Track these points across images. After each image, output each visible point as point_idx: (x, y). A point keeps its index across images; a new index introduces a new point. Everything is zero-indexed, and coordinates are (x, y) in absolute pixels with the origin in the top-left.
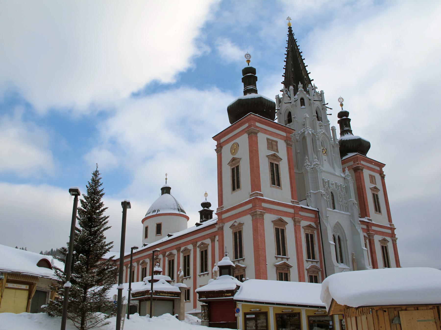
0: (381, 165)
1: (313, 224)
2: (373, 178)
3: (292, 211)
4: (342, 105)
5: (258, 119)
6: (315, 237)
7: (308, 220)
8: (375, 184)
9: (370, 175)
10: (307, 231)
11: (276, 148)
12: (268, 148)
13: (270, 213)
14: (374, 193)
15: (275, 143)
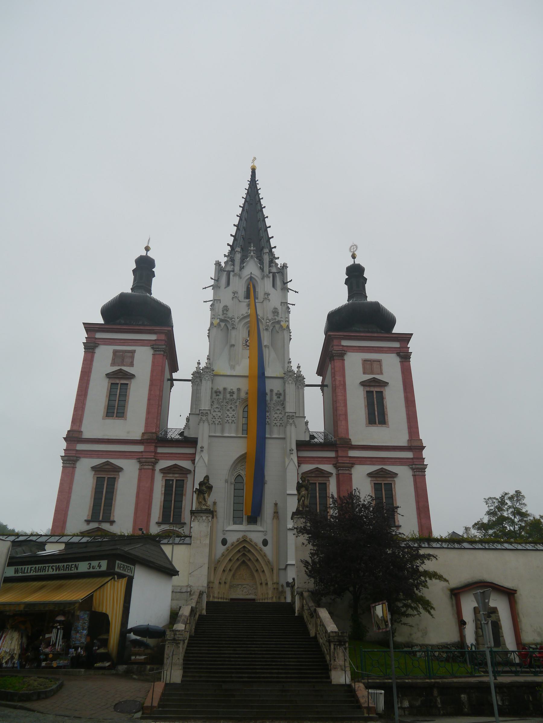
0: (406, 338)
1: (185, 464)
2: (375, 365)
3: (140, 448)
4: (354, 257)
5: (99, 328)
6: (187, 484)
7: (176, 458)
8: (378, 374)
9: (365, 361)
10: (171, 475)
11: (130, 360)
12: (113, 364)
13: (91, 457)
14: (372, 389)
15: (130, 354)
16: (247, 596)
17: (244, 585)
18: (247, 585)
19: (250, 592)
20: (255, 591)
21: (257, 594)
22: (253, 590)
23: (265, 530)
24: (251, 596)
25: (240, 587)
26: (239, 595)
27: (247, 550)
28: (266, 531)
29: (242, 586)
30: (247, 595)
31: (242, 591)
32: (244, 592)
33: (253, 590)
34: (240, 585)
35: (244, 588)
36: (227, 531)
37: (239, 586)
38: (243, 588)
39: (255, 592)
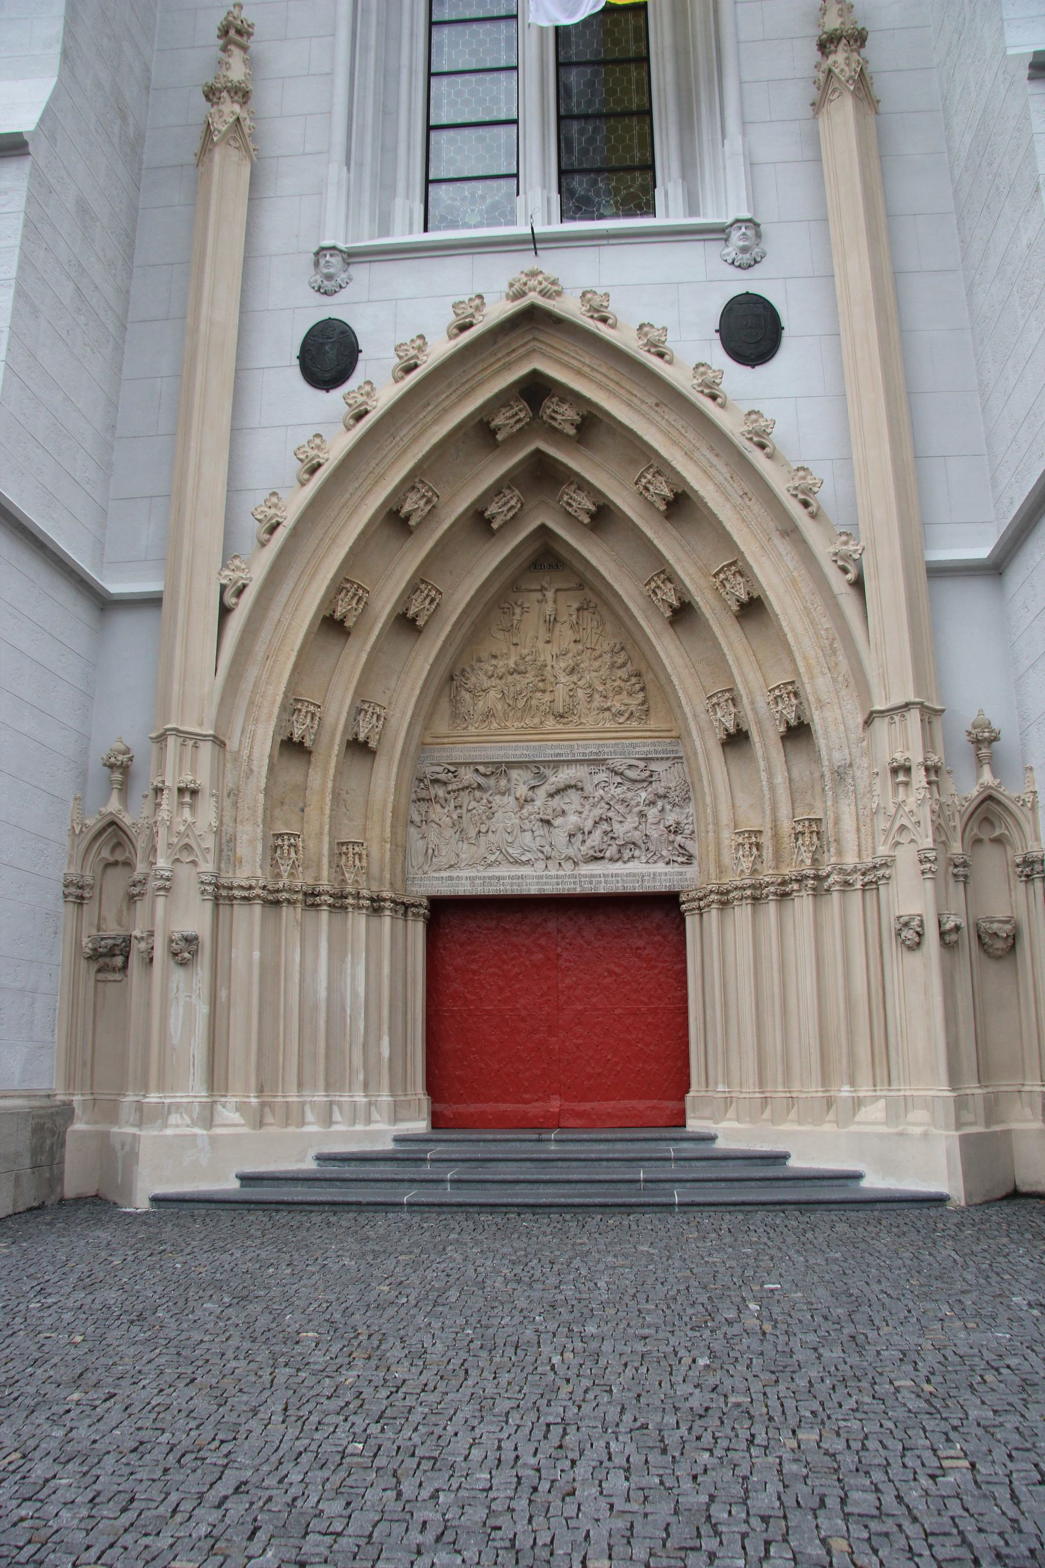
16: (586, 869)
17: (556, 764)
18: (596, 762)
19: (619, 830)
20: (671, 818)
21: (692, 847)
22: (652, 812)
23: (746, 215)
24: (634, 867)
25: (522, 791)
26: (517, 862)
27: (566, 415)
28: (752, 223)
29: (544, 778)
30: (596, 859)
31: (548, 822)
32: (560, 837)
33: (652, 812)
34: (511, 765)
35: (558, 791)
36: (352, 257)
37: (514, 774)
38: (552, 795)
39: (676, 830)
